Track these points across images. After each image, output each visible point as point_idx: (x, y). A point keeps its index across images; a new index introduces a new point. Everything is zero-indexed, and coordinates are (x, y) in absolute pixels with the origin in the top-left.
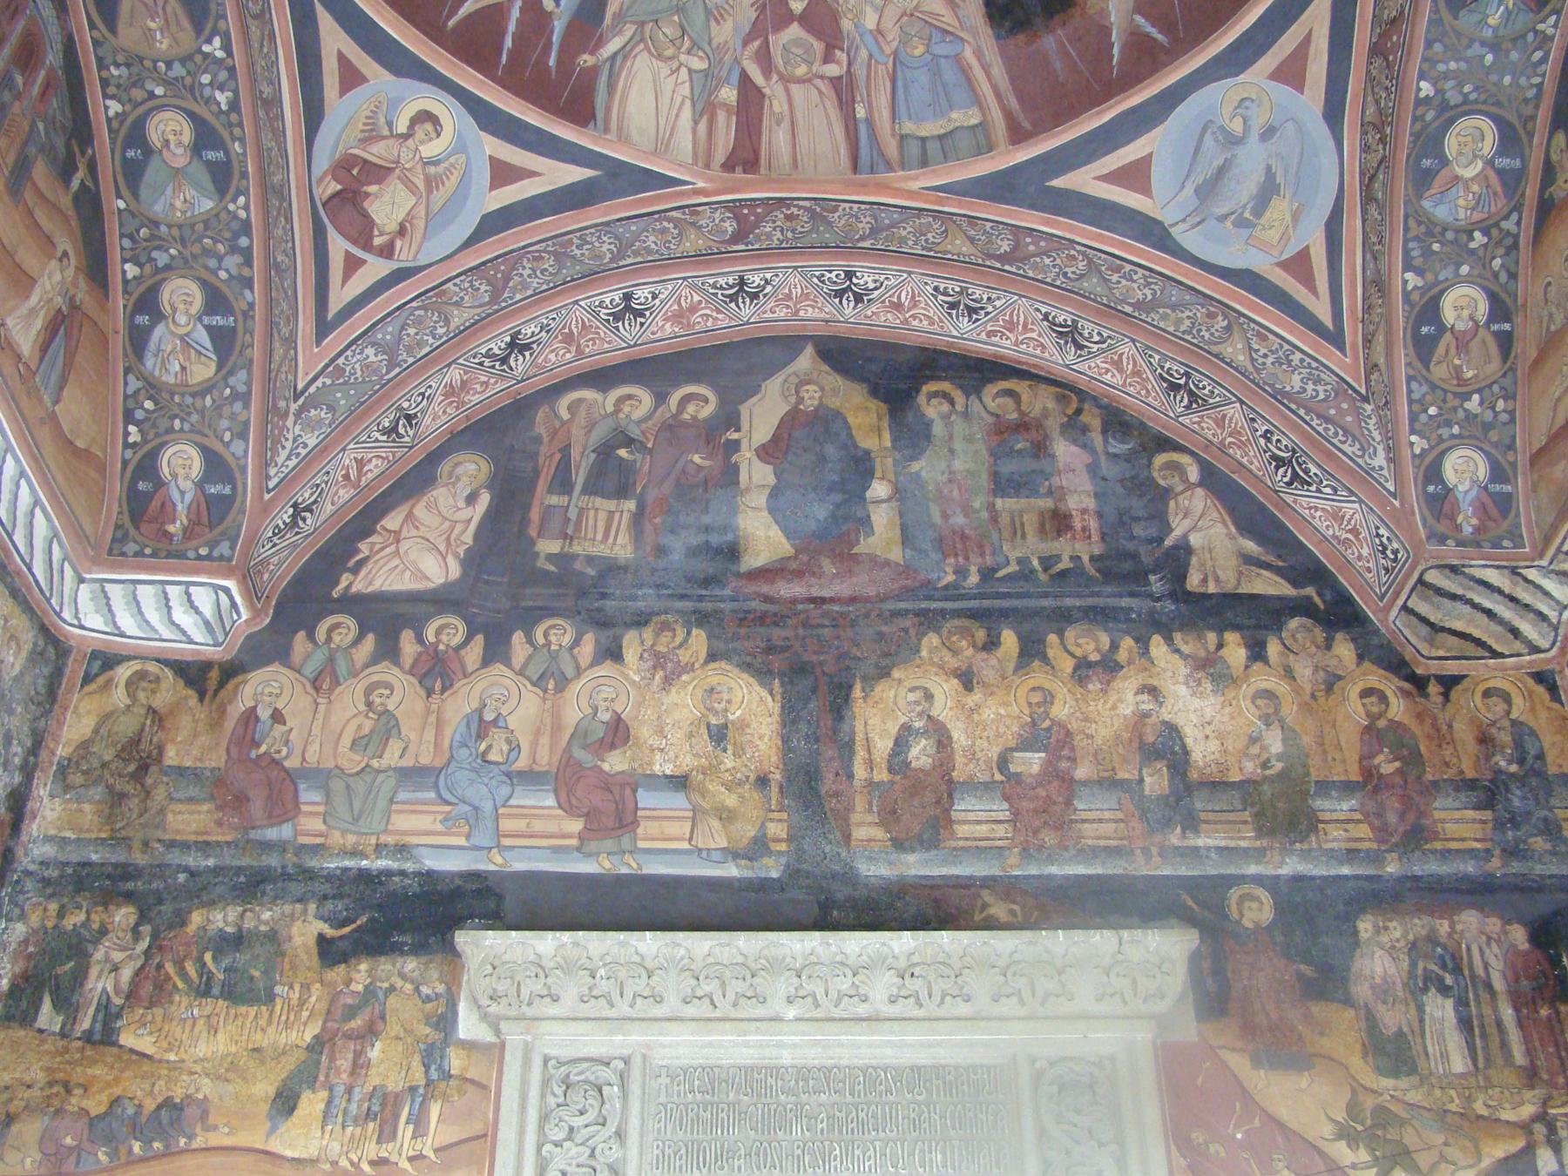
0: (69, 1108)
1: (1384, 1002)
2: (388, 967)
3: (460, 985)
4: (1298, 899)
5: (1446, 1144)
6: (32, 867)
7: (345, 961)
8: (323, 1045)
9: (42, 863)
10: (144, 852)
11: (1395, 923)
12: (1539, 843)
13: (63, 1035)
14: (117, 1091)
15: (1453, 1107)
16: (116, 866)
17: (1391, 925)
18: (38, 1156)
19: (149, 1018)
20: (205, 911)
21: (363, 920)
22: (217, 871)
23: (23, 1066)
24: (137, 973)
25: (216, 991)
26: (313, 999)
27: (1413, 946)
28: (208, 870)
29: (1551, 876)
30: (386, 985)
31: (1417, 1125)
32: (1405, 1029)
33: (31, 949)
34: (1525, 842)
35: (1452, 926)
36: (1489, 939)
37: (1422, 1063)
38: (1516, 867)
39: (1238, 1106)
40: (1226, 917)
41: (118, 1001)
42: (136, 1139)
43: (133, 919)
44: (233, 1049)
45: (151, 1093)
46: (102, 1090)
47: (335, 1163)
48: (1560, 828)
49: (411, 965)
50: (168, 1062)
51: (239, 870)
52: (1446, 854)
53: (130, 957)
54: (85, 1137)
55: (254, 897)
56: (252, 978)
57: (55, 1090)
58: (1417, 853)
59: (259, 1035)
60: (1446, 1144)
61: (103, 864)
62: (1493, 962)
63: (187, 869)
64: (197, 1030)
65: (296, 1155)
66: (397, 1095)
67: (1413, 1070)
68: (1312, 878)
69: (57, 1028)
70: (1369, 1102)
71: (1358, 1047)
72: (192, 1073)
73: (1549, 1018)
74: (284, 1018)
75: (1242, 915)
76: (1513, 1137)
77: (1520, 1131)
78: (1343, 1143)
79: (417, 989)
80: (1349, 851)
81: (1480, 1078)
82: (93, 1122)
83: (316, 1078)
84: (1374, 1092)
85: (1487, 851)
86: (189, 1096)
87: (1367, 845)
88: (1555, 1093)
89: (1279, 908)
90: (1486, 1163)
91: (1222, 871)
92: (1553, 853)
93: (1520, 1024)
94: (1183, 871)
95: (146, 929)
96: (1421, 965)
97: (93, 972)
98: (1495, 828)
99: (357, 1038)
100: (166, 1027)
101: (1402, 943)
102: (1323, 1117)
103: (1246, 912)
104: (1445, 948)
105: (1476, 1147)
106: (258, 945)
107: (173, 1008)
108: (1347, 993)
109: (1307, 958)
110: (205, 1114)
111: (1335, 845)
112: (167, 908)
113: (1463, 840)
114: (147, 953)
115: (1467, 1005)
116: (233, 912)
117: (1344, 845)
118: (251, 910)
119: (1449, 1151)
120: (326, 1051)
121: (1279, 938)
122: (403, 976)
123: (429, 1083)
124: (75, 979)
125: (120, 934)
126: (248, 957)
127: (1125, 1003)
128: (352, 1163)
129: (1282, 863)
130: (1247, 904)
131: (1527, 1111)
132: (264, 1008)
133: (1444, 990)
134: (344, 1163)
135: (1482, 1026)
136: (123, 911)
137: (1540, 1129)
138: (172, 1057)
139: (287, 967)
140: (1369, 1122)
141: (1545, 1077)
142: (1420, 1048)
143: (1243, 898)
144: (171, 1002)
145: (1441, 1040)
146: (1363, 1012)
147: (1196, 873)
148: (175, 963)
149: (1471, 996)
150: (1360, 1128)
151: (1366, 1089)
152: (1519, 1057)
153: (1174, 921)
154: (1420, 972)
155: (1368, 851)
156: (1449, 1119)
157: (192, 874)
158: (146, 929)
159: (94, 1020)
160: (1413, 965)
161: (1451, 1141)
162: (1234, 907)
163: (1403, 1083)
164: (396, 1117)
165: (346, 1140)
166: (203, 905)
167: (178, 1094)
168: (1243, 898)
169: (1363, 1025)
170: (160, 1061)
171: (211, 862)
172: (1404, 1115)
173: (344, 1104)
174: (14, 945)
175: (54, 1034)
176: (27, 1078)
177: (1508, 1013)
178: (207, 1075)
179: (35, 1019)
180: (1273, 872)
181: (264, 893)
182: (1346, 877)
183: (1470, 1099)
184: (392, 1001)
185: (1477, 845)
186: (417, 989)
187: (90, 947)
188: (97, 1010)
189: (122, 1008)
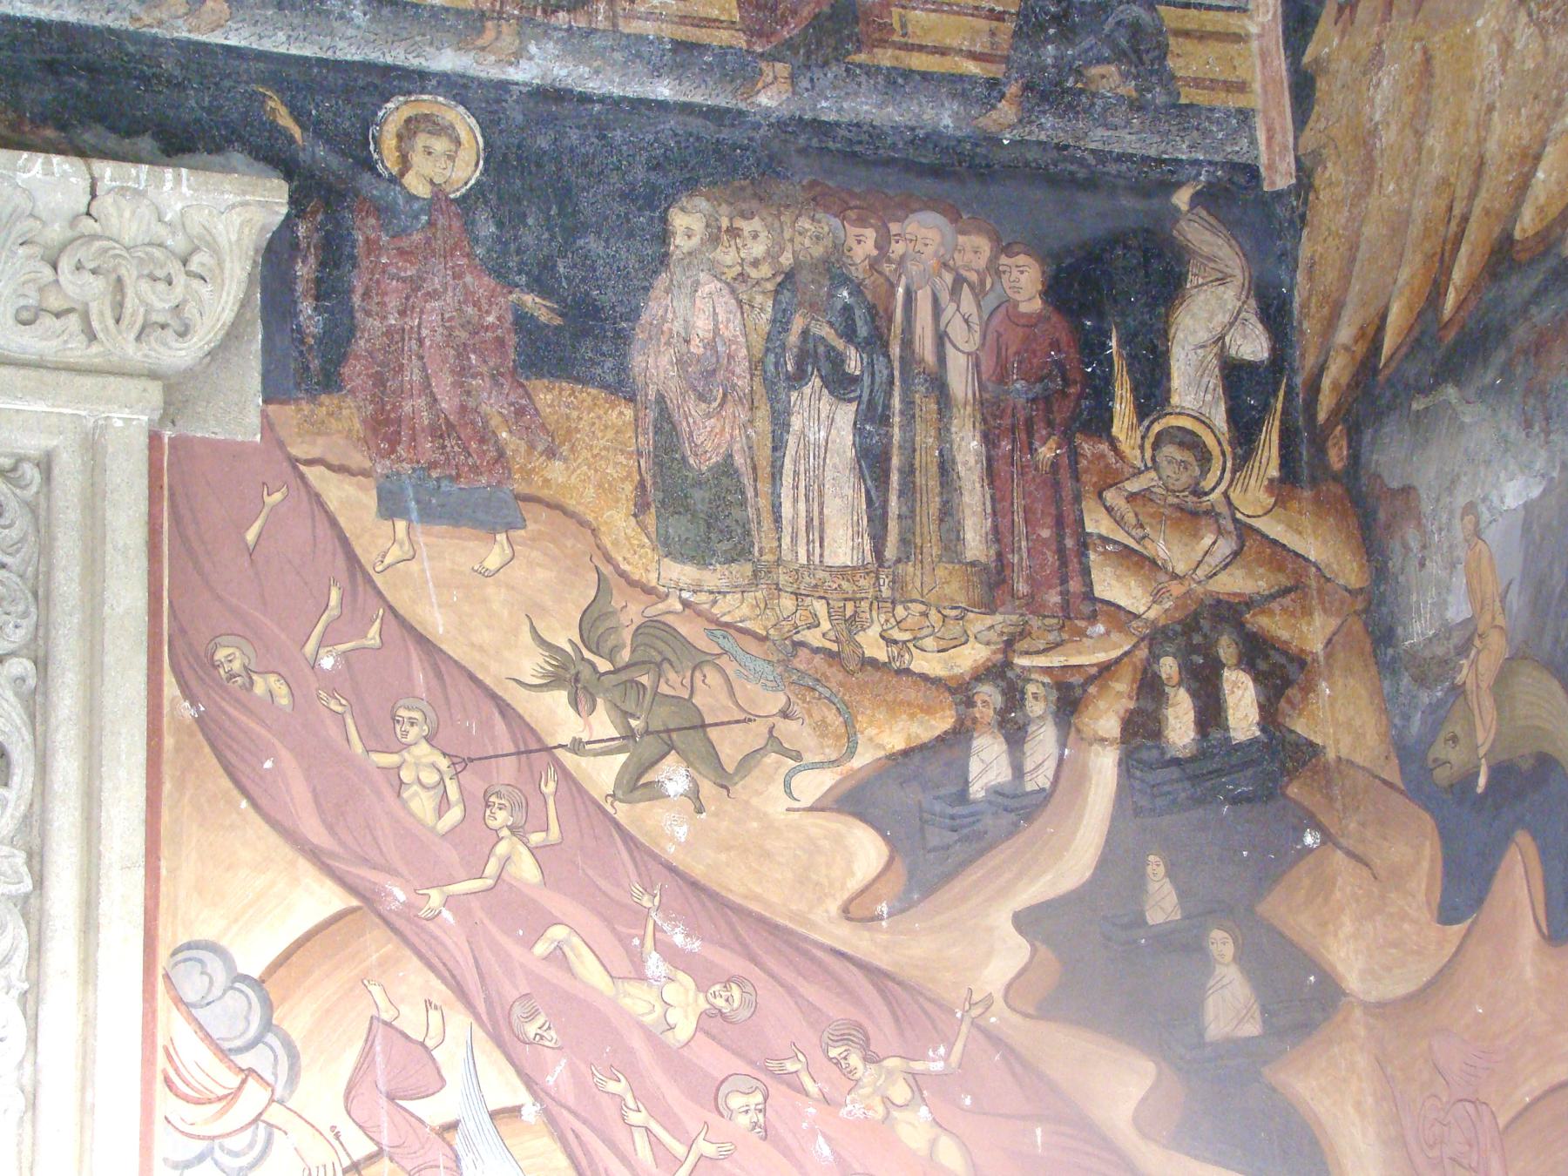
1: (701, 397)
4: (543, 142)
5: (785, 714)
11: (756, 224)
12: (1110, 79)
15: (814, 638)
17: (747, 226)
27: (788, 279)
29: (1120, 158)
31: (731, 669)
32: (739, 460)
34: (1079, 73)
35: (882, 245)
36: (959, 281)
37: (763, 539)
38: (1049, 127)
39: (335, 595)
40: (369, 165)
48: (1163, 52)
52: (897, 81)
58: (835, 69)
60: (785, 714)
62: (957, 330)
67: (741, 552)
68: (585, 99)
70: (632, 612)
71: (629, 487)
73: (1055, 465)
75: (405, 163)
76: (928, 710)
77: (948, 699)
78: (561, 696)
80: (679, 46)
81: (885, 581)
84: (648, 591)
85: (993, 83)
87: (722, 37)
88: (1035, 622)
89: (496, 159)
90: (864, 758)
91: (374, 56)
92: (1137, 106)
93: (991, 474)
94: (278, 43)
96: (798, 324)
98: (1017, 34)
101: (765, 270)
102: (526, 636)
103: (417, 158)
104: (857, 290)
105: (849, 724)
108: (622, 368)
109: (541, 283)
111: (649, 28)
113: (942, 51)
115: (885, 420)
117: (669, 31)
119: (786, 728)
121: (487, 229)
127: (92, 337)
129: (519, 55)
130: (422, 140)
131: (971, 656)
133: (840, 384)
135: (909, 471)
137: (989, 696)
140: (625, 655)
141: (1022, 588)
142: (763, 503)
143: (411, 127)
145: (815, 494)
146: (652, 415)
147: (308, 51)
149: (896, 402)
150: (604, 666)
151: (633, 584)
152: (975, 542)
153: (238, 158)
154: (793, 338)
155: (724, 51)
156: (802, 661)
160: (781, 323)
161: (797, 709)
162: (389, 142)
163: (714, 577)
168: (411, 127)
169: (647, 441)
172: (703, 643)
177: (968, 447)
180: (495, 73)
182: (662, 105)
183: (853, 623)
185: (972, 68)
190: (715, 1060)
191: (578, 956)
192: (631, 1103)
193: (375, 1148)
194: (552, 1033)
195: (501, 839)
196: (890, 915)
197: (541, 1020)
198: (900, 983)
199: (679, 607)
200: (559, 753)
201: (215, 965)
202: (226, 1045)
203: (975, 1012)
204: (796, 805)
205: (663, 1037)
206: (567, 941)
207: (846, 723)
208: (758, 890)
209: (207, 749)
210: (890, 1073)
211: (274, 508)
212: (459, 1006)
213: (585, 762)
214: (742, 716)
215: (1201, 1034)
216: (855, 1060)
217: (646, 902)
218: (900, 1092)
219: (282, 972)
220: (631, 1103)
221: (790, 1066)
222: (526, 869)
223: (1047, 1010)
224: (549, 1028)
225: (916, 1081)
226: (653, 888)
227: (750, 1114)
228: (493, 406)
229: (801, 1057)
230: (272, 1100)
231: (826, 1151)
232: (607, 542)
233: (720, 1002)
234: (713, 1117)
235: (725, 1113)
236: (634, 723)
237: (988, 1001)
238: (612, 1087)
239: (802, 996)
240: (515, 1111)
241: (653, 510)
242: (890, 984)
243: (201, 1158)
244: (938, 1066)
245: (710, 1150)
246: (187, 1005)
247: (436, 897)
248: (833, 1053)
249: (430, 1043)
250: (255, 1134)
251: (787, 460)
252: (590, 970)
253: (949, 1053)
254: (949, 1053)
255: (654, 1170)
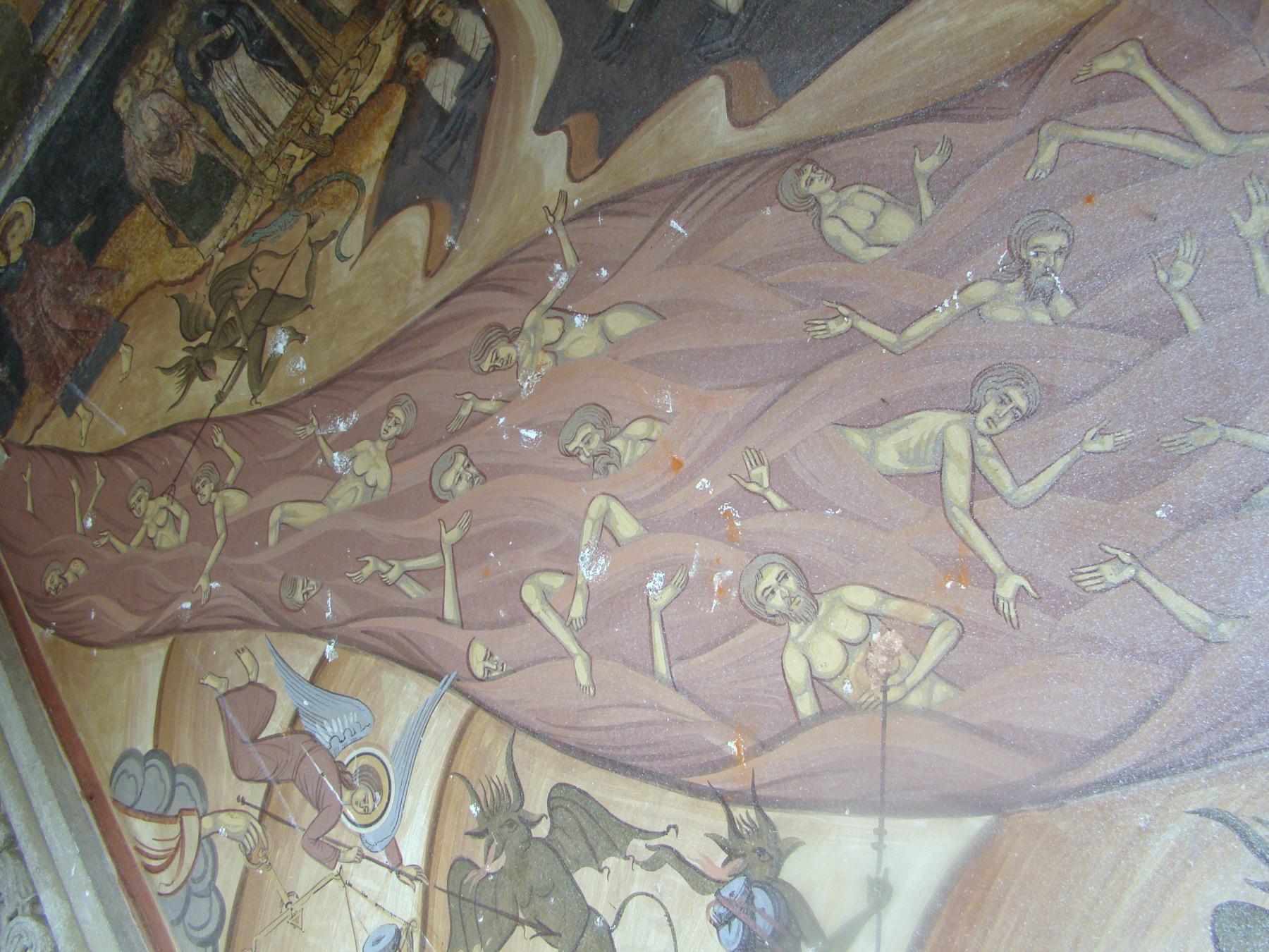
39: (74, 484)
60: (311, 224)
90: (371, 182)
119: (318, 233)
137: (416, 51)
190: (415, 471)
191: (294, 515)
192: (383, 567)
193: (264, 786)
194: (312, 582)
195: (213, 504)
196: (456, 239)
197: (300, 583)
198: (497, 265)
199: (221, 255)
200: (214, 414)
201: (133, 766)
202: (161, 810)
203: (559, 217)
204: (354, 259)
205: (374, 499)
206: (284, 514)
207: (348, 180)
208: (367, 334)
209: (66, 643)
210: (535, 328)
211: (31, 481)
212: (253, 632)
213: (228, 401)
214: (289, 258)
215: (727, 15)
216: (504, 351)
217: (310, 431)
218: (552, 329)
219: (162, 728)
220: (383, 567)
221: (465, 412)
222: (237, 500)
223: (607, 148)
224: (308, 581)
225: (560, 311)
226: (307, 416)
227: (464, 477)
228: (87, 296)
229: (467, 397)
230: (200, 818)
231: (532, 434)
232: (169, 278)
233: (393, 431)
234: (443, 510)
235: (446, 498)
236: (239, 344)
237: (564, 198)
238: (367, 571)
239: (437, 360)
240: (323, 660)
241: (180, 231)
242: (490, 275)
243: (187, 902)
244: (564, 279)
245: (452, 536)
246: (131, 807)
247: (203, 582)
248: (486, 367)
249: (252, 678)
250: (204, 851)
251: (227, 115)
252: (307, 514)
253: (564, 264)
254: (564, 264)
255: (430, 595)
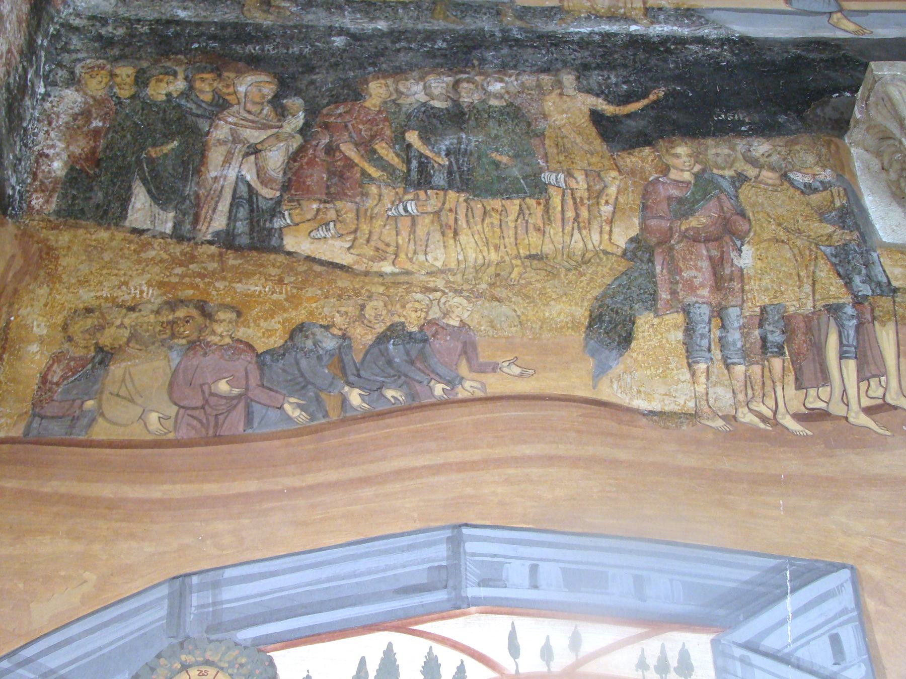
0: (215, 339)
2: (724, 150)
3: (854, 175)
6: (76, 22)
7: (648, 143)
8: (651, 251)
9: (93, 18)
10: (267, 12)
13: (178, 236)
14: (299, 315)
16: (222, 26)
18: (173, 410)
19: (332, 214)
20: (390, 81)
21: (658, 93)
22: (395, 35)
23: (115, 281)
24: (294, 157)
25: (440, 179)
26: (612, 190)
28: (382, 35)
30: (728, 173)
33: (97, 123)
41: (268, 193)
42: (350, 384)
43: (269, 89)
44: (494, 256)
45: (361, 317)
46: (271, 314)
47: (731, 419)
49: (761, 147)
50: (381, 275)
51: (431, 36)
53: (277, 136)
54: (254, 381)
55: (467, 63)
56: (497, 164)
57: (181, 313)
59: (534, 238)
61: (198, 24)
63: (341, 32)
64: (421, 231)
65: (656, 406)
66: (808, 319)
69: (168, 228)
72: (427, 290)
74: (570, 214)
79: (785, 176)
82: (262, 360)
83: (654, 296)
86: (432, 323)
95: (295, 103)
97: (216, 156)
99: (707, 240)
100: (365, 228)
106: (491, 123)
107: (370, 203)
110: (468, 349)
112: (325, 79)
114: (302, 131)
116: (439, 84)
118: (468, 81)
120: (658, 260)
122: (753, 162)
123: (858, 302)
124: (185, 164)
125: (254, 109)
126: (481, 138)
128: (764, 419)
132: (531, 202)
134: (746, 417)
136: (250, 79)
138: (387, 268)
139: (552, 151)
144: (365, 195)
148: (357, 145)
157: (355, 37)
158: (295, 103)
159: (232, 217)
164: (819, 350)
165: (739, 385)
166: (385, 74)
167: (413, 323)
170: (367, 274)
171: (382, 25)
173: (716, 333)
174: (64, 118)
175: (163, 235)
176: (124, 296)
178: (458, 292)
179: (123, 215)
181: (483, 61)
184: (746, 193)
186: (785, 176)
187: (204, 125)
188: (235, 203)
189: (279, 202)
